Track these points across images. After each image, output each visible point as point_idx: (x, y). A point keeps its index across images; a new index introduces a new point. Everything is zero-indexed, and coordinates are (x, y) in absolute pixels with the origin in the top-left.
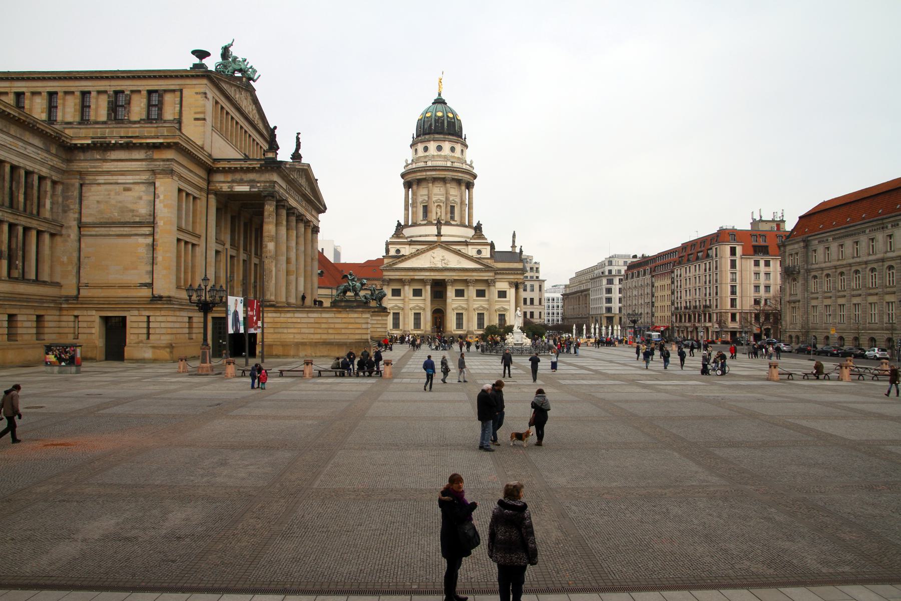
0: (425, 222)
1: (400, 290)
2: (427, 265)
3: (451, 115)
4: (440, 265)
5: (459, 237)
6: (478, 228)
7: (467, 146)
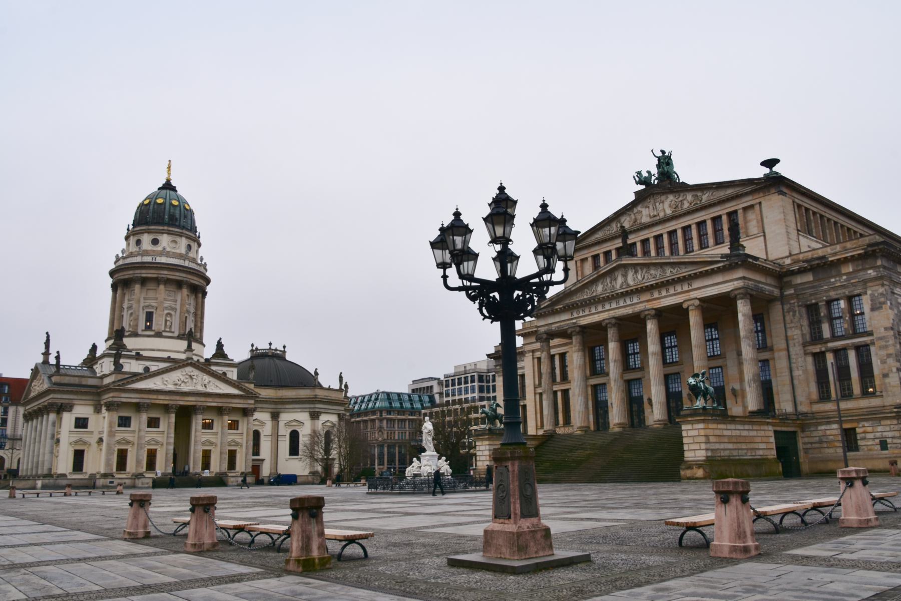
0: (152, 333)
1: (159, 419)
6: (220, 345)
7: (199, 245)
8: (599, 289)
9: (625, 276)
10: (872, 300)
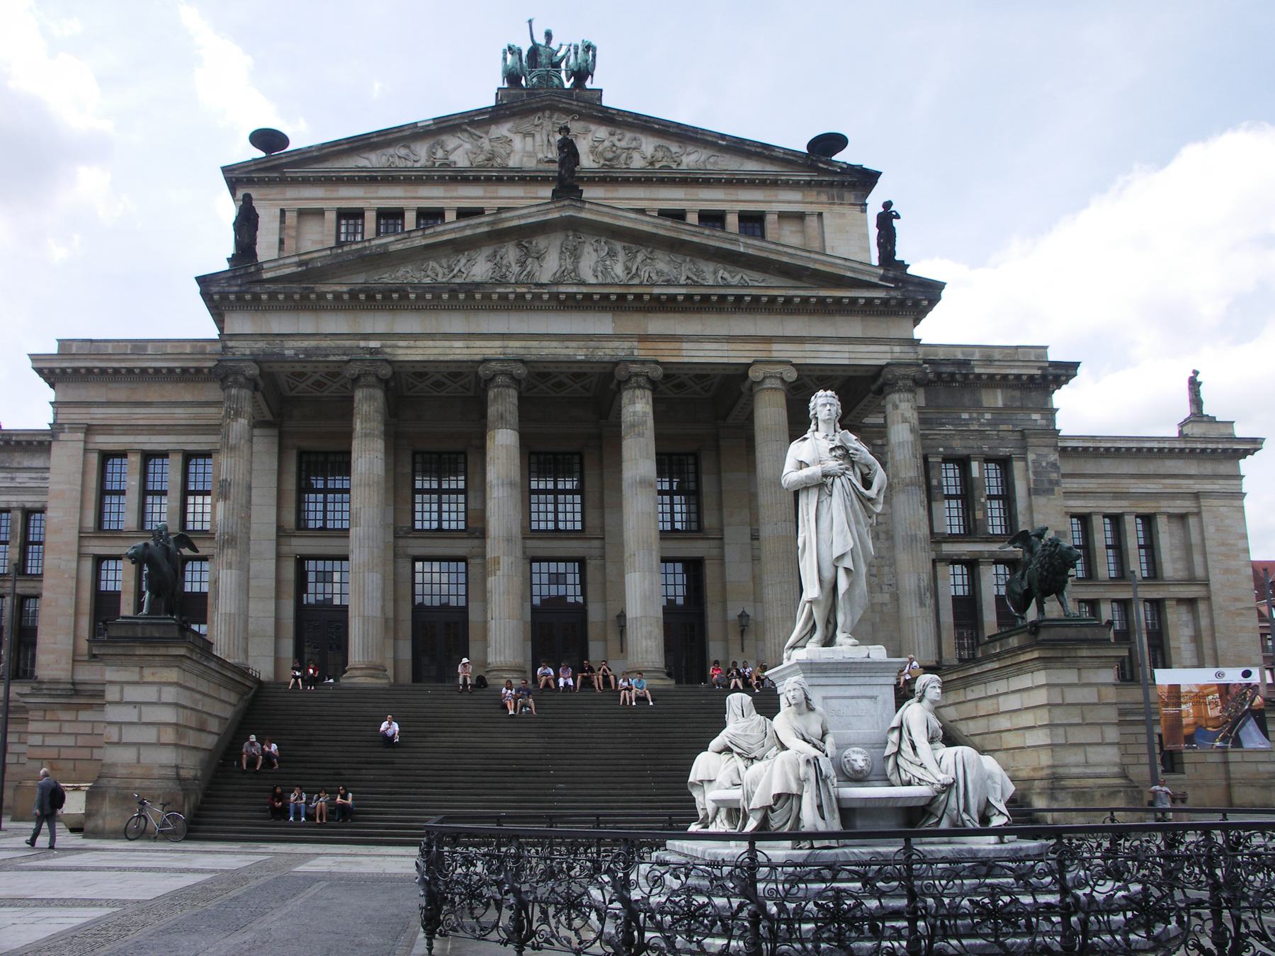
8: (479, 269)
9: (575, 254)
10: (1035, 473)
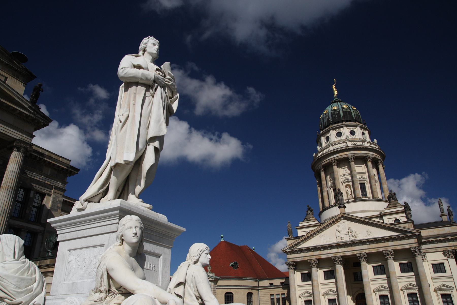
2: (333, 241)
3: (345, 107)
4: (347, 239)
5: (374, 211)
